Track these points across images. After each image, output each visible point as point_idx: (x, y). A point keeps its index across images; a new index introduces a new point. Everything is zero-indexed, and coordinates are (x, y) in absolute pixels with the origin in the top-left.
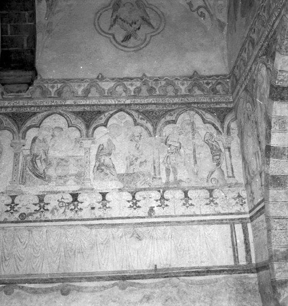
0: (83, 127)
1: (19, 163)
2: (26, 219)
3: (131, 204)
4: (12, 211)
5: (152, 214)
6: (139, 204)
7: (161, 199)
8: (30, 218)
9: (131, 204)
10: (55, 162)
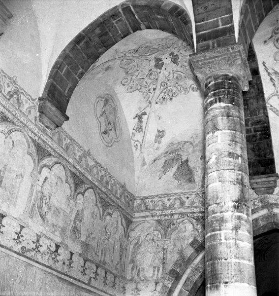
0: (73, 188)
1: (32, 196)
2: (25, 254)
4: (18, 241)
8: (28, 254)
10: (53, 209)
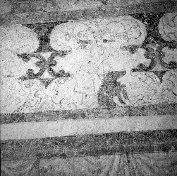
3: (32, 64)
5: (116, 100)
6: (62, 64)
7: (146, 42)
9: (32, 64)
